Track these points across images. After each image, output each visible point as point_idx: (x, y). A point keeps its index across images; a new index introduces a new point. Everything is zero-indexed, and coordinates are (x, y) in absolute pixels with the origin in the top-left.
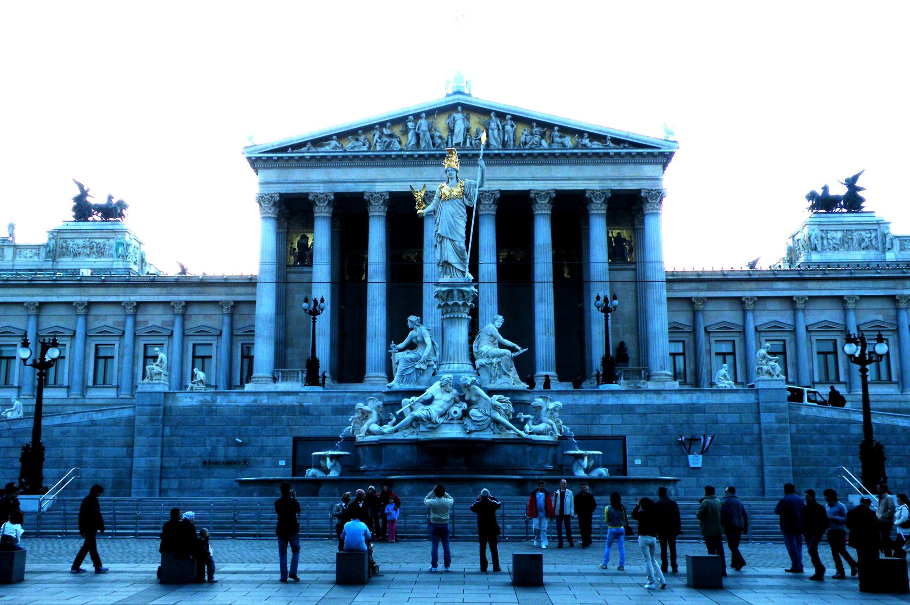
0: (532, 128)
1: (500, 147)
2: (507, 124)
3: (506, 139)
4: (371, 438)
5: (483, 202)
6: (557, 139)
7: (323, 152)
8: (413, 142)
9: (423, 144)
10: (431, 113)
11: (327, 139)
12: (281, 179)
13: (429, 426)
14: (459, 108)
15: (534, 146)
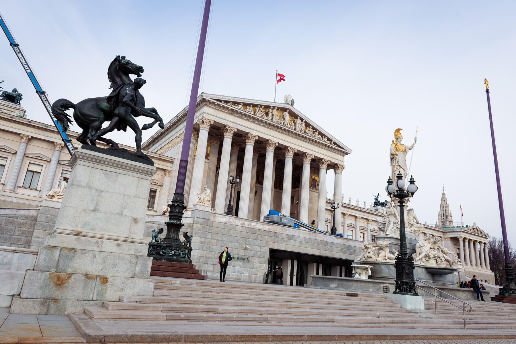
0: (309, 128)
1: (300, 131)
2: (303, 123)
3: (302, 129)
4: (389, 261)
5: (290, 152)
6: (316, 135)
7: (237, 109)
8: (271, 118)
9: (274, 120)
10: (278, 108)
11: (239, 103)
12: (215, 114)
13: (427, 259)
14: (288, 111)
15: (311, 136)
